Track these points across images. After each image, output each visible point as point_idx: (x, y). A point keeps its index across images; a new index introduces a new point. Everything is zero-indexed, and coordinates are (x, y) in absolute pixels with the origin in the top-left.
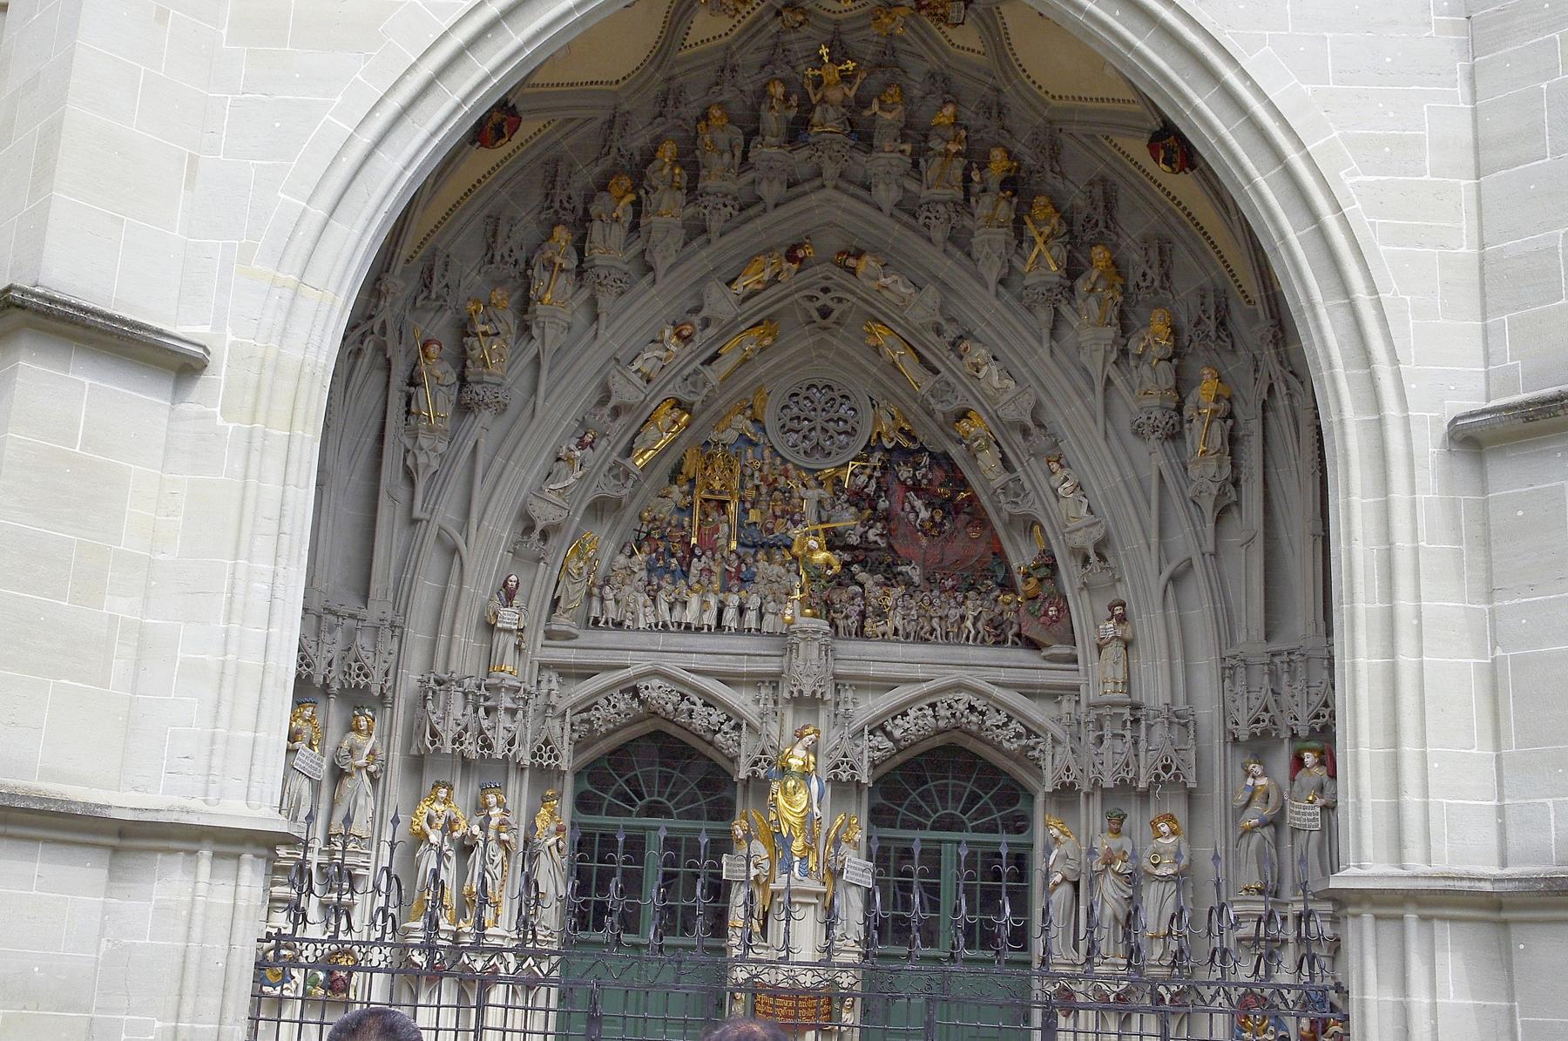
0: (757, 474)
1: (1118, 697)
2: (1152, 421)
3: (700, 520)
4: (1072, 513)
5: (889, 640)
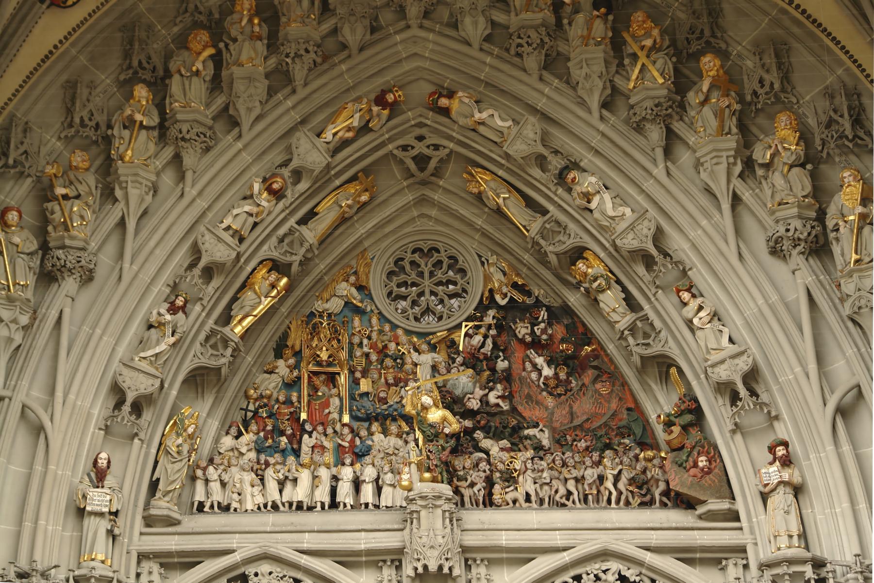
0: (365, 341)
1: (797, 552)
2: (790, 234)
3: (309, 395)
4: (712, 344)
5: (521, 507)
